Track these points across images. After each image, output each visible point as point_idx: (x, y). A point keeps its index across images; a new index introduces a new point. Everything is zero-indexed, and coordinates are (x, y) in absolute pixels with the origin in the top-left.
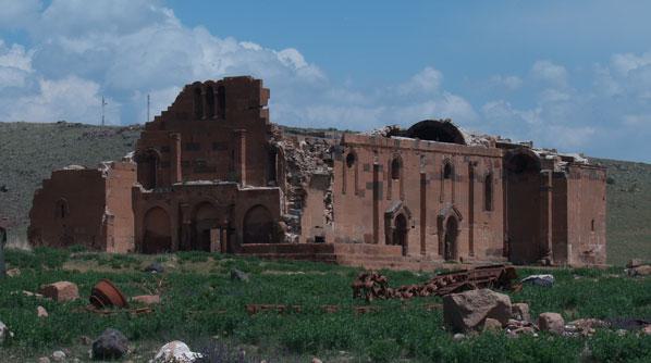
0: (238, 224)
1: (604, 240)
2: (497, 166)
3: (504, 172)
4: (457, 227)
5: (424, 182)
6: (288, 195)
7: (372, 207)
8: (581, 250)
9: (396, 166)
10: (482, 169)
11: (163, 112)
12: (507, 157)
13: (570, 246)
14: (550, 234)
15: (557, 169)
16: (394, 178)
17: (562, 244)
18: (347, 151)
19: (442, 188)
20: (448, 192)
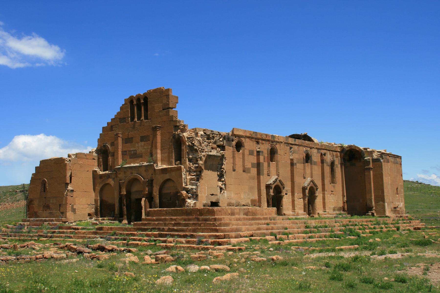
0: (156, 194)
1: (403, 200)
2: (337, 157)
3: (341, 161)
4: (315, 193)
5: (292, 164)
6: (190, 171)
7: (256, 181)
8: (393, 206)
9: (273, 153)
10: (329, 158)
11: (111, 119)
12: (341, 152)
13: (386, 204)
14: (373, 197)
15: (375, 157)
16: (272, 161)
17: (381, 203)
18: (236, 140)
19: (304, 169)
20: (308, 171)
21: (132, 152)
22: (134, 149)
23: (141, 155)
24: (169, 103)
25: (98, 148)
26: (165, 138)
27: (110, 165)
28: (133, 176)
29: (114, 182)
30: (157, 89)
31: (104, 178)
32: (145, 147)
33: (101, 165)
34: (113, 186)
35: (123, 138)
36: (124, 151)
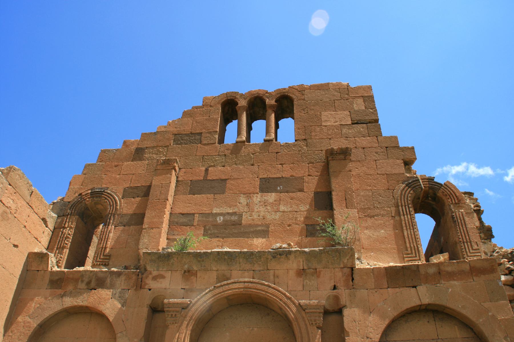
21: (220, 219)
22: (231, 211)
23: (260, 228)
24: (376, 110)
25: (65, 200)
26: (369, 188)
27: (108, 250)
28: (242, 285)
29: (123, 306)
30: (328, 84)
31: (70, 288)
32: (282, 208)
33: (64, 248)
34: (111, 319)
35: (180, 179)
36: (183, 214)
